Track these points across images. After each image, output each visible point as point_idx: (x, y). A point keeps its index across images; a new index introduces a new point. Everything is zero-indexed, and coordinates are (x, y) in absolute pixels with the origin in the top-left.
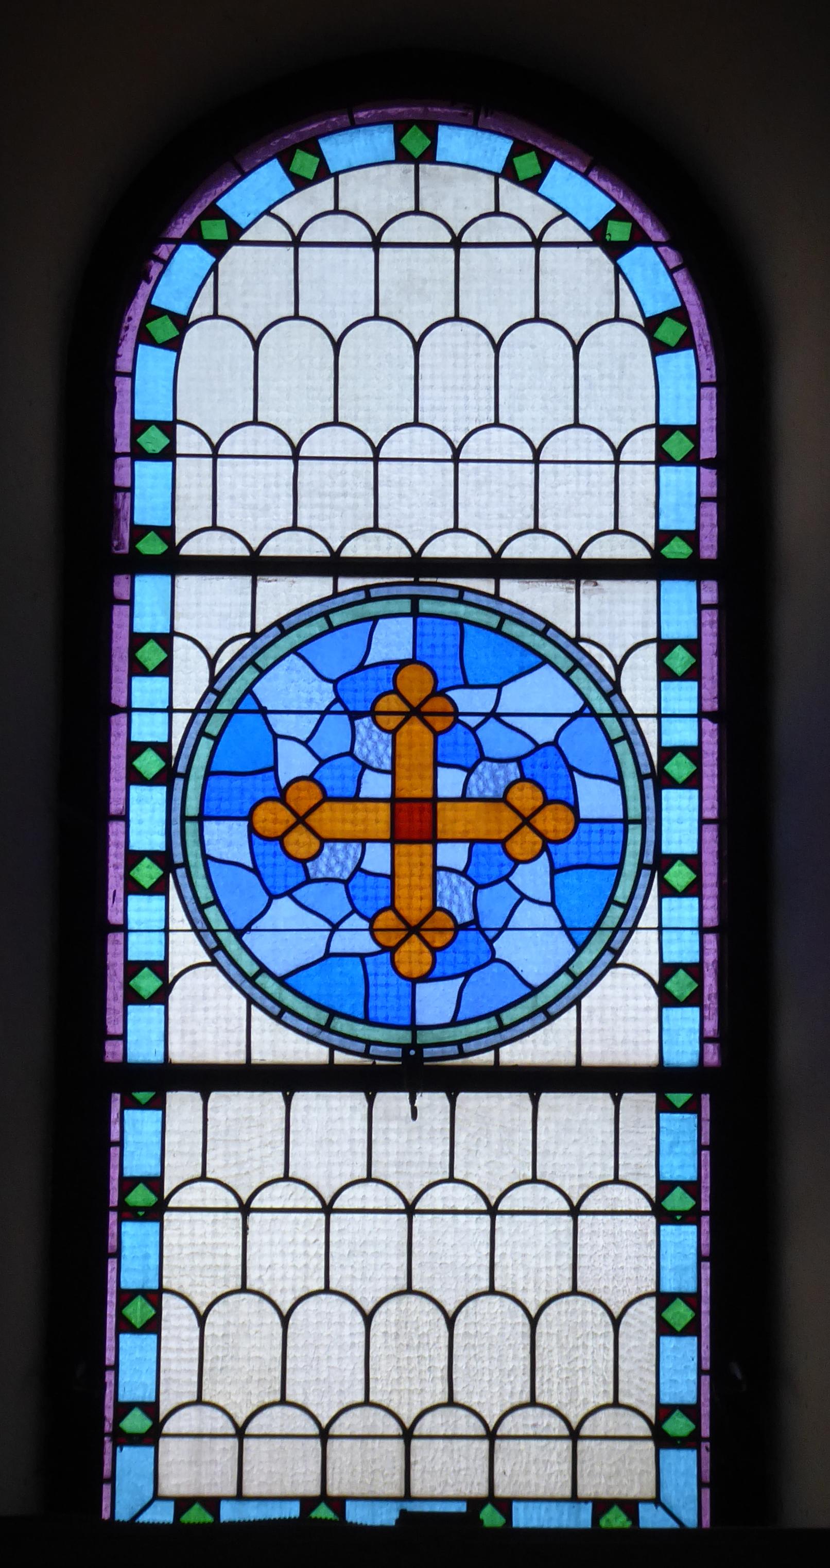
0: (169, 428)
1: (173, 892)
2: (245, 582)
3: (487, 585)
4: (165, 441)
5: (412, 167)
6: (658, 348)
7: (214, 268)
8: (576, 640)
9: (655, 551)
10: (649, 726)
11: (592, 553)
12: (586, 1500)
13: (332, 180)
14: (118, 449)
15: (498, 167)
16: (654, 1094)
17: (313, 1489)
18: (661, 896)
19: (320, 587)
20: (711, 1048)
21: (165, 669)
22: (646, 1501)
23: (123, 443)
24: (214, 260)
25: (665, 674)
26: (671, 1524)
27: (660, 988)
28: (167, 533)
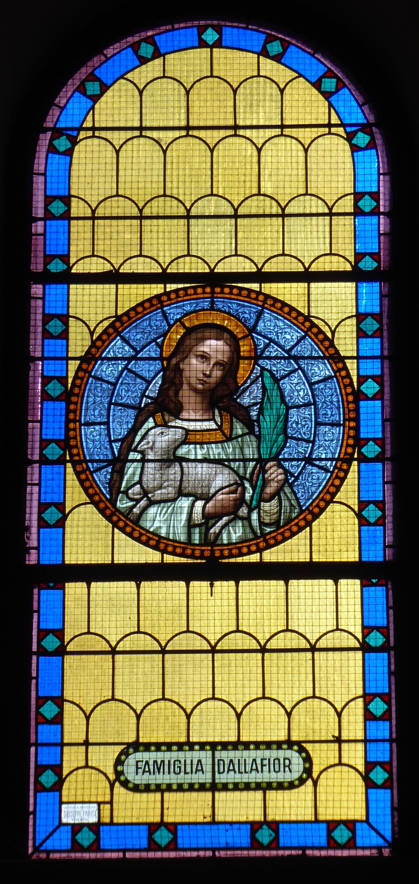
3: (255, 286)
5: (209, 49)
6: (355, 149)
9: (355, 266)
15: (259, 49)
16: (358, 582)
19: (157, 289)
21: (64, 335)
24: (92, 104)
25: (361, 334)
28: (65, 258)
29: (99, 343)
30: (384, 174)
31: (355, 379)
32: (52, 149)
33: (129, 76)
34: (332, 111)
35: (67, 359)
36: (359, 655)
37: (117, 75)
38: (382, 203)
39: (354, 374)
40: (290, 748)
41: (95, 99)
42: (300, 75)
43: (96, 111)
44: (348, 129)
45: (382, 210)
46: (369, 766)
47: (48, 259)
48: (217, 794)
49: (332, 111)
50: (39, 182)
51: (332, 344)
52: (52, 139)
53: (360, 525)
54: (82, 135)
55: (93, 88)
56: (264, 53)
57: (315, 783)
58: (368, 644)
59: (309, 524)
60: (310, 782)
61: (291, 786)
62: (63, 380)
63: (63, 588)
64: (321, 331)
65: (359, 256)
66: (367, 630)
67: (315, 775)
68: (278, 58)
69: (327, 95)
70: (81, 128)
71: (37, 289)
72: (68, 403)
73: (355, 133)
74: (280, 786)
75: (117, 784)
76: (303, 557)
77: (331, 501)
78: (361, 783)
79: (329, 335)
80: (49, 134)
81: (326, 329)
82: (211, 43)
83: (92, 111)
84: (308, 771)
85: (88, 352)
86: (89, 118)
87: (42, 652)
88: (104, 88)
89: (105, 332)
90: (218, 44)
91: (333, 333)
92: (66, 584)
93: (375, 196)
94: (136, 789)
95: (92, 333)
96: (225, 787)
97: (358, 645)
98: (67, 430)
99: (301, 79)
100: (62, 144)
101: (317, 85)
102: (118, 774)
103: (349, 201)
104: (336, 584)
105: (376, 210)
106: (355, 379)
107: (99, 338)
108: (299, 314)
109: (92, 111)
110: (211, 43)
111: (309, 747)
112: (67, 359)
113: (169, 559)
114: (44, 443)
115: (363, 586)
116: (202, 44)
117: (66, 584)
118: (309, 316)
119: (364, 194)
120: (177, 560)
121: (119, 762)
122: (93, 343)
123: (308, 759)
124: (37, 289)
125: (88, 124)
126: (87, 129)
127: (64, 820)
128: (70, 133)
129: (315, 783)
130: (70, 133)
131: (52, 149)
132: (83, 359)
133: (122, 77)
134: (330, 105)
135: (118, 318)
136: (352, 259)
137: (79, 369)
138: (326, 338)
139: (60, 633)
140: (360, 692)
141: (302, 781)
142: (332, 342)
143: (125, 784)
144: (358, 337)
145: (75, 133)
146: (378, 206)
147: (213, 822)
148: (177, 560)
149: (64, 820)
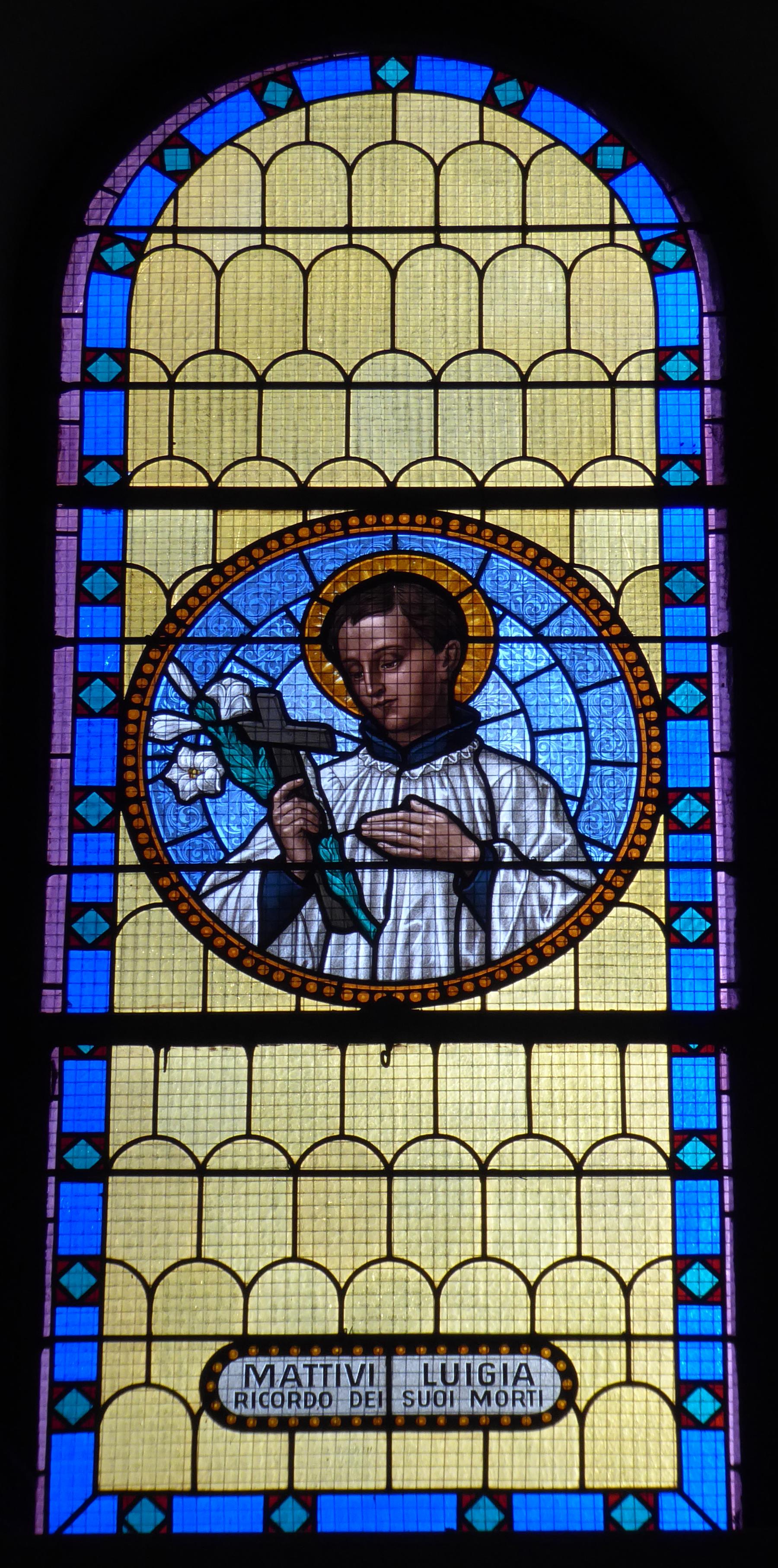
0: (122, 355)
1: (123, 833)
2: (204, 516)
4: (117, 368)
5: (390, 96)
6: (656, 270)
7: (174, 196)
8: (570, 568)
9: (657, 479)
10: (652, 653)
11: (585, 481)
12: (594, 1491)
13: (302, 112)
14: (65, 378)
16: (663, 1048)
17: (278, 1481)
18: (667, 833)
20: (724, 994)
21: (117, 598)
22: (668, 1490)
23: (70, 371)
26: (699, 1525)
27: (667, 929)
28: (119, 462)
29: (182, 613)
30: (709, 314)
31: (658, 679)
32: (98, 266)
33: (242, 140)
34: (617, 205)
35: (122, 641)
36: (665, 1183)
37: (221, 139)
38: (707, 365)
39: (656, 670)
40: (536, 1350)
41: (180, 178)
42: (558, 142)
43: (181, 201)
44: (647, 235)
45: (707, 377)
46: (684, 1387)
47: (87, 463)
48: (395, 1435)
49: (617, 205)
50: (72, 329)
51: (616, 619)
52: (100, 248)
53: (669, 946)
54: (156, 240)
55: (177, 159)
56: (488, 100)
57: (581, 1416)
58: (682, 1163)
59: (573, 943)
60: (572, 1417)
61: (537, 1422)
62: (113, 679)
63: (108, 1058)
64: (595, 593)
65: (665, 461)
66: (679, 1137)
67: (582, 1398)
68: (516, 110)
69: (607, 176)
70: (153, 229)
71: (66, 518)
72: (124, 721)
73: (656, 242)
74: (516, 1423)
75: (206, 1421)
76: (563, 1003)
77: (616, 903)
78: (669, 1420)
79: (611, 600)
80: (94, 237)
81: (603, 589)
82: (393, 84)
83: (172, 202)
84: (569, 1394)
85: (161, 629)
86: (169, 212)
87: (66, 1173)
88: (198, 159)
89: (194, 592)
90: (408, 85)
91: (617, 594)
92: (114, 1048)
93: (694, 353)
94: (241, 1424)
95: (169, 594)
96: (411, 1424)
97: (662, 1165)
98: (122, 768)
99: (559, 148)
100: (118, 256)
101: (589, 159)
102: (209, 1396)
103: (648, 361)
104: (622, 1052)
105: (697, 378)
106: (658, 679)
107: (183, 603)
108: (557, 561)
109: (172, 202)
110: (393, 84)
111: (571, 1349)
112: (122, 641)
113: (309, 1005)
114: (78, 794)
115: (671, 1055)
116: (379, 86)
117: (114, 1048)
118: (572, 564)
119: (674, 350)
120: (324, 1007)
121: (210, 1375)
122: (171, 613)
123: (569, 1374)
124: (66, 518)
125: (166, 220)
126: (164, 230)
127: (106, 1482)
128: (133, 236)
129: (581, 1416)
130: (133, 236)
131: (98, 266)
132: (150, 642)
133: (230, 142)
134: (614, 195)
135: (217, 568)
136: (652, 466)
137: (145, 658)
138: (605, 605)
139: (100, 1140)
140: (668, 1251)
141: (557, 1414)
142: (614, 612)
143: (222, 1417)
144: (664, 605)
145: (142, 237)
146: (701, 371)
147: (389, 1490)
148: (324, 1007)
149: (106, 1482)
